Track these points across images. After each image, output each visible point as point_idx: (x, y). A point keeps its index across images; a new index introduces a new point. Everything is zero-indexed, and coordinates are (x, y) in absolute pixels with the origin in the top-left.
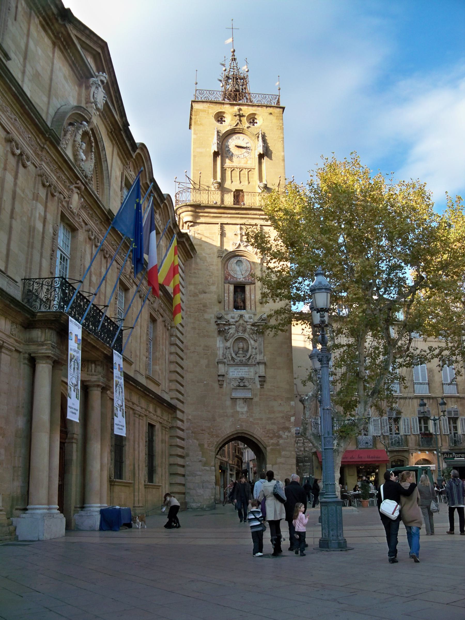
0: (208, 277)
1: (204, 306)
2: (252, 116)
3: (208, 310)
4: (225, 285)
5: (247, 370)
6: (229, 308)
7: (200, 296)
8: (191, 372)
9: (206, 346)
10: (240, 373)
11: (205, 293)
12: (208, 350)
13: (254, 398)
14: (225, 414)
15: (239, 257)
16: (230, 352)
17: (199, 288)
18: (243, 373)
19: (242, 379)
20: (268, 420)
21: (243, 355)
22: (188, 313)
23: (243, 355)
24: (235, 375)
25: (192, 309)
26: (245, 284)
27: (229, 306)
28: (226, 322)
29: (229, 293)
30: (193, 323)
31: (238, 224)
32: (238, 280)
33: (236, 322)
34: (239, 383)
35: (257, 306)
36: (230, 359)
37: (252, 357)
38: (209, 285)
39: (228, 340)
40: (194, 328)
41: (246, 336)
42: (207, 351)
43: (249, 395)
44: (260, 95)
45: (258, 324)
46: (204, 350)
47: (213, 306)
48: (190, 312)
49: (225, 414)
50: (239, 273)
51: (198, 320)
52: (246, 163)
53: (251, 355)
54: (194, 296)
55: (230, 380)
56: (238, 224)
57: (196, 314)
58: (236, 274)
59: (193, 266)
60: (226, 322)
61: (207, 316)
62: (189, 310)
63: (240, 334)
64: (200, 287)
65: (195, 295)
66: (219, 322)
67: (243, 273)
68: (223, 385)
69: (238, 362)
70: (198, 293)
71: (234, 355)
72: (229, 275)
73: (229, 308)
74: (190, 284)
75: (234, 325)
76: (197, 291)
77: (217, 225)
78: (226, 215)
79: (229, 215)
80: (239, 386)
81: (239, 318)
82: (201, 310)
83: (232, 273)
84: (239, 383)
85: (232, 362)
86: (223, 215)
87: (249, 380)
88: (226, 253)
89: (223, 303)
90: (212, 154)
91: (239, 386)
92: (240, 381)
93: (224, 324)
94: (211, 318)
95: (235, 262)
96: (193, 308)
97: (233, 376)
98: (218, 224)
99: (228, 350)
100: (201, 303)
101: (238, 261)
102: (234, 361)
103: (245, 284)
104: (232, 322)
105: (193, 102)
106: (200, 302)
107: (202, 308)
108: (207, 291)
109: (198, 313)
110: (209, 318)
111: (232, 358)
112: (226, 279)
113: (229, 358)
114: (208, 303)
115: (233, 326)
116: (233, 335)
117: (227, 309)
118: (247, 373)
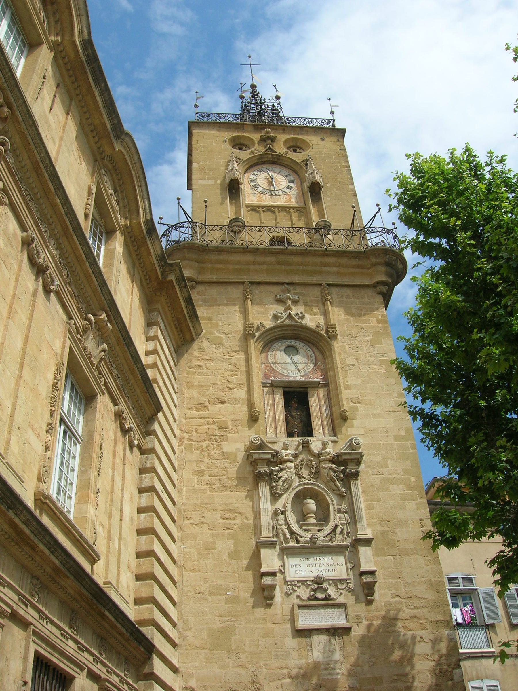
0: (229, 373)
1: (220, 428)
2: (291, 144)
3: (229, 435)
4: (264, 389)
5: (328, 562)
6: (276, 434)
7: (210, 408)
8: (193, 570)
9: (230, 511)
10: (314, 569)
11: (222, 403)
12: (234, 519)
13: (354, 627)
14: (285, 671)
15: (289, 341)
16: (286, 520)
17: (207, 393)
18: (322, 568)
19: (318, 581)
20: (394, 681)
21: (318, 528)
22: (186, 442)
23: (318, 528)
24: (303, 574)
25: (194, 433)
26: (307, 388)
27: (276, 428)
28: (272, 455)
29: (274, 405)
30: (197, 461)
31: (282, 284)
32: (291, 379)
33: (296, 456)
34: (313, 590)
35: (336, 425)
36: (288, 536)
37: (339, 530)
38: (230, 388)
39: (280, 496)
40: (201, 473)
41: (320, 486)
42: (233, 522)
43: (341, 622)
44: (302, 120)
45: (345, 457)
46: (223, 519)
47: (240, 428)
48: (189, 439)
49: (285, 671)
50: (292, 367)
51: (209, 456)
52: (289, 201)
53: (336, 526)
54: (197, 409)
55: (292, 584)
56: (282, 284)
57: (204, 444)
58: (286, 369)
59: (196, 354)
60: (272, 455)
61: (227, 447)
62: (186, 435)
63: (307, 481)
64: (211, 391)
65: (201, 406)
66: (256, 457)
67: (300, 367)
68: (272, 598)
69: (307, 542)
70: (207, 404)
71: (295, 527)
72: (272, 370)
73: (276, 434)
74: (190, 385)
75: (291, 461)
76: (205, 399)
77: (241, 287)
78: (257, 267)
79: (265, 267)
80: (316, 599)
81: (301, 447)
82: (214, 435)
83: (278, 368)
84: (314, 590)
85: (292, 544)
86: (252, 267)
87: (335, 582)
88: (263, 330)
89: (261, 421)
90: (226, 185)
91: (316, 599)
92: (316, 586)
93: (269, 462)
94: (238, 449)
95: (283, 348)
96: (196, 431)
97: (299, 575)
98: (243, 283)
99: (282, 517)
100: (214, 423)
101: (287, 347)
102: (298, 542)
103: (307, 388)
104: (287, 455)
105: (192, 125)
106: (211, 420)
107: (217, 432)
108: (226, 399)
109: (208, 442)
110: (234, 451)
111: (292, 533)
112: (266, 376)
113: (284, 534)
114: (229, 422)
115: (289, 464)
116: (290, 486)
117: (274, 436)
118: (331, 568)
